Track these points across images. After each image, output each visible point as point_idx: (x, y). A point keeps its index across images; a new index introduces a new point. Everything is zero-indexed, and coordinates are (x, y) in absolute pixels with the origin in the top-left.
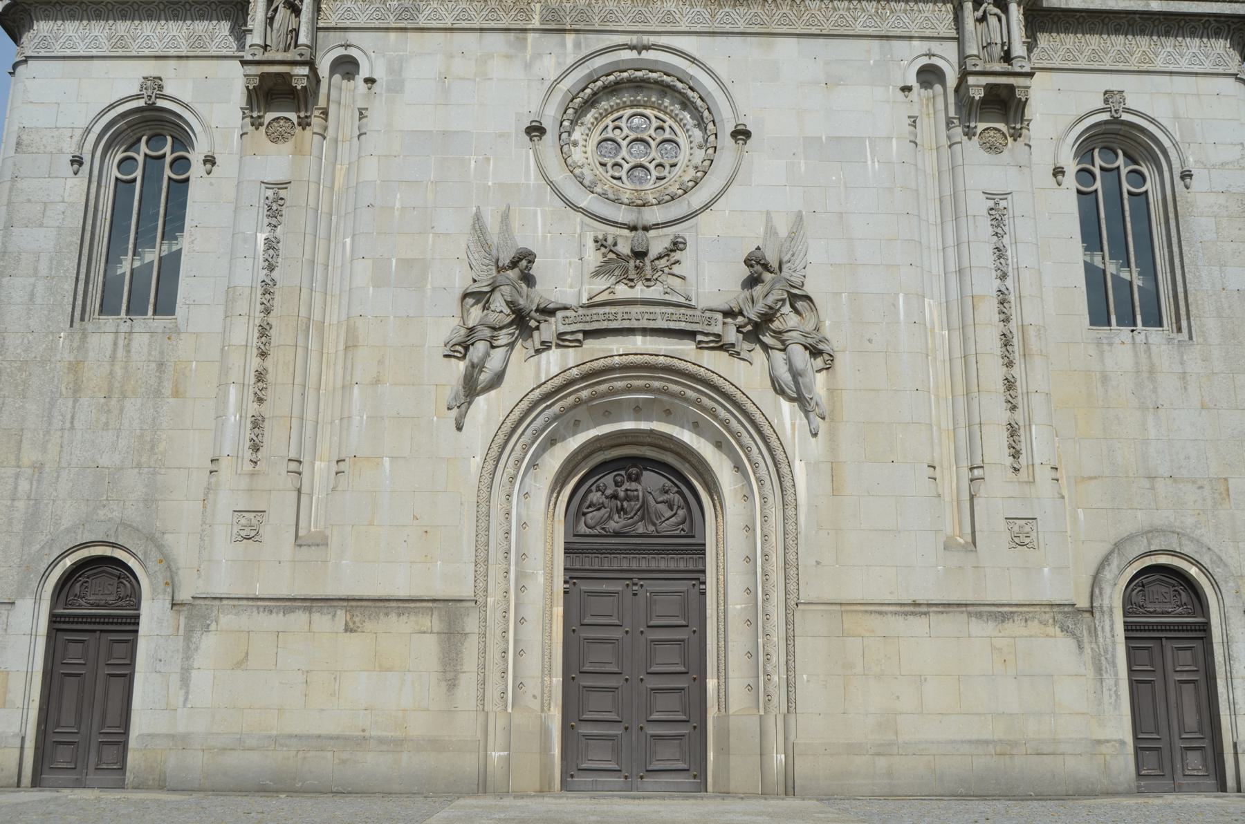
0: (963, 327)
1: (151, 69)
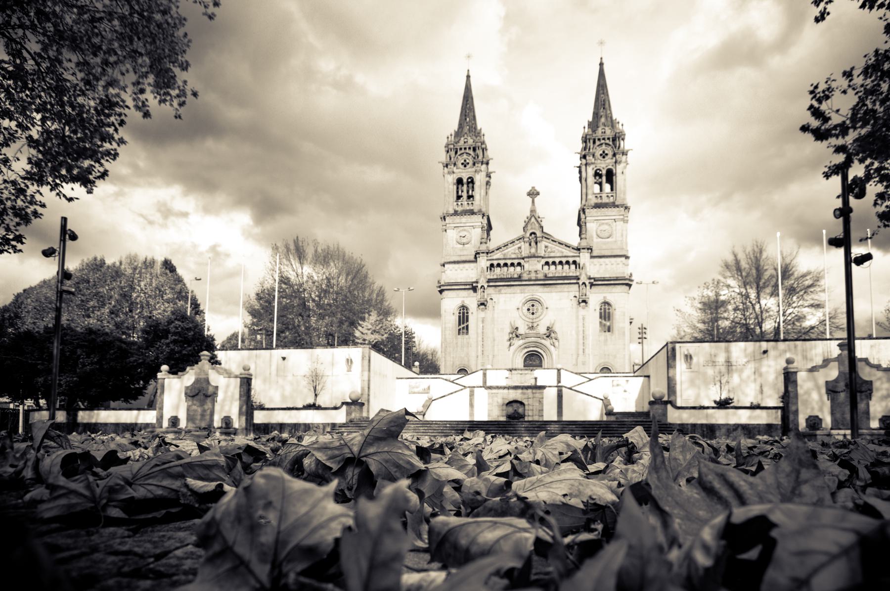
0: (577, 334)
1: (462, 299)
